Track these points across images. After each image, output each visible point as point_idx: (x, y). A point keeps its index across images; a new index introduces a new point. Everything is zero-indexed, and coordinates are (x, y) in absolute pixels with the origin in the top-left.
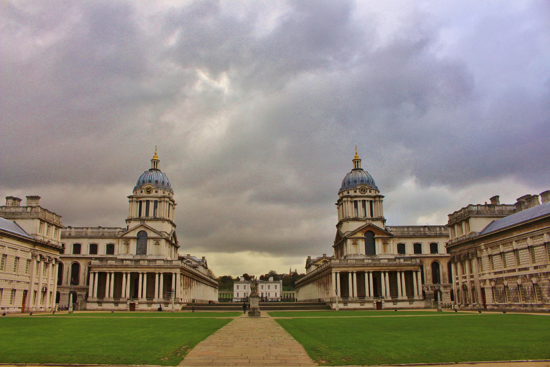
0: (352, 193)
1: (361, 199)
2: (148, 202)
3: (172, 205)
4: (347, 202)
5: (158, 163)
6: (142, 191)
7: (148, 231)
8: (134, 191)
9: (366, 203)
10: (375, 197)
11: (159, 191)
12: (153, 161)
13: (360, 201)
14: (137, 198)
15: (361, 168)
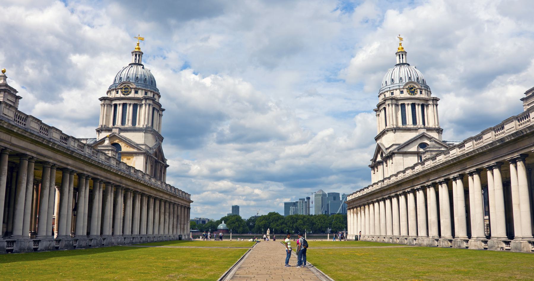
0: (397, 94)
1: (410, 102)
2: (124, 105)
3: (158, 111)
4: (392, 105)
5: (140, 56)
6: (118, 91)
7: (122, 144)
8: (108, 93)
9: (417, 106)
10: (427, 100)
11: (140, 92)
12: (134, 53)
13: (408, 104)
14: (111, 100)
15: (407, 63)
